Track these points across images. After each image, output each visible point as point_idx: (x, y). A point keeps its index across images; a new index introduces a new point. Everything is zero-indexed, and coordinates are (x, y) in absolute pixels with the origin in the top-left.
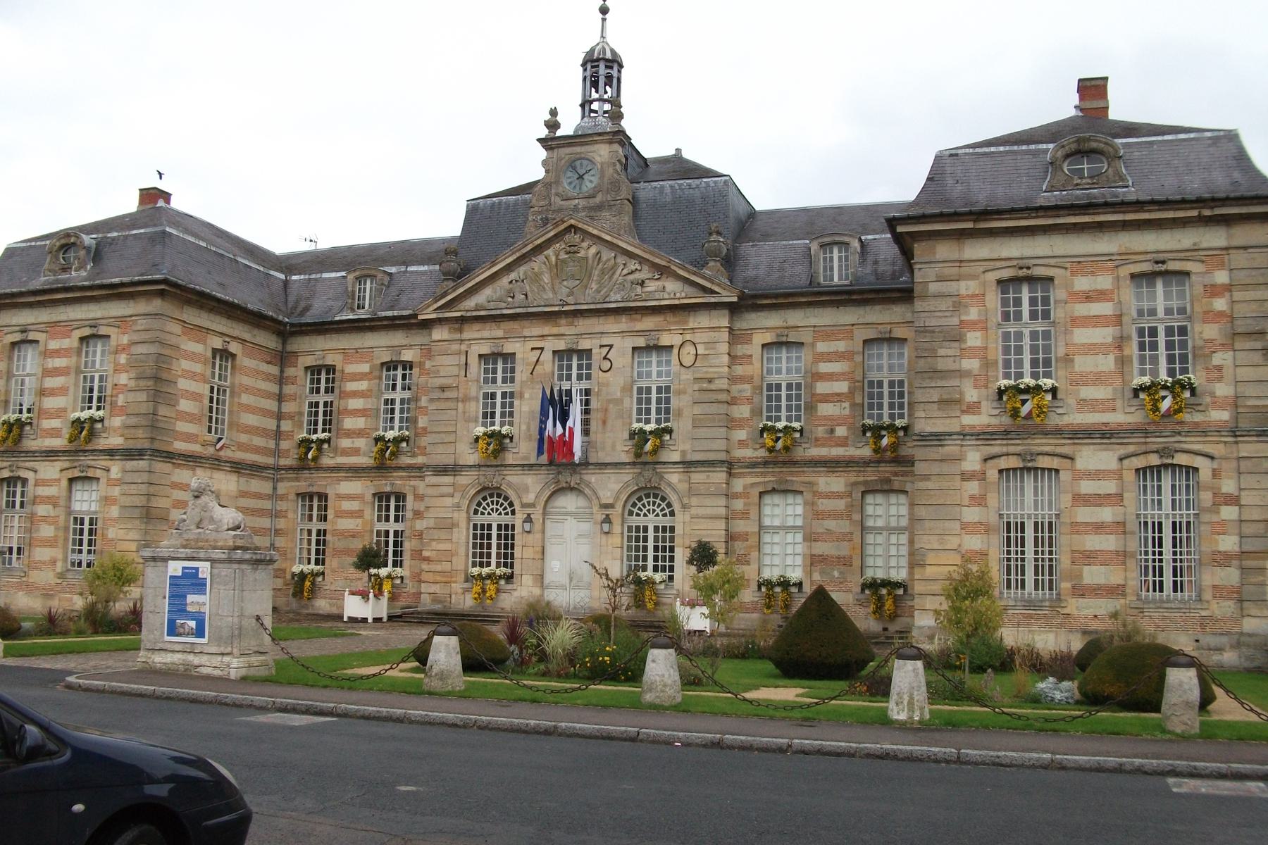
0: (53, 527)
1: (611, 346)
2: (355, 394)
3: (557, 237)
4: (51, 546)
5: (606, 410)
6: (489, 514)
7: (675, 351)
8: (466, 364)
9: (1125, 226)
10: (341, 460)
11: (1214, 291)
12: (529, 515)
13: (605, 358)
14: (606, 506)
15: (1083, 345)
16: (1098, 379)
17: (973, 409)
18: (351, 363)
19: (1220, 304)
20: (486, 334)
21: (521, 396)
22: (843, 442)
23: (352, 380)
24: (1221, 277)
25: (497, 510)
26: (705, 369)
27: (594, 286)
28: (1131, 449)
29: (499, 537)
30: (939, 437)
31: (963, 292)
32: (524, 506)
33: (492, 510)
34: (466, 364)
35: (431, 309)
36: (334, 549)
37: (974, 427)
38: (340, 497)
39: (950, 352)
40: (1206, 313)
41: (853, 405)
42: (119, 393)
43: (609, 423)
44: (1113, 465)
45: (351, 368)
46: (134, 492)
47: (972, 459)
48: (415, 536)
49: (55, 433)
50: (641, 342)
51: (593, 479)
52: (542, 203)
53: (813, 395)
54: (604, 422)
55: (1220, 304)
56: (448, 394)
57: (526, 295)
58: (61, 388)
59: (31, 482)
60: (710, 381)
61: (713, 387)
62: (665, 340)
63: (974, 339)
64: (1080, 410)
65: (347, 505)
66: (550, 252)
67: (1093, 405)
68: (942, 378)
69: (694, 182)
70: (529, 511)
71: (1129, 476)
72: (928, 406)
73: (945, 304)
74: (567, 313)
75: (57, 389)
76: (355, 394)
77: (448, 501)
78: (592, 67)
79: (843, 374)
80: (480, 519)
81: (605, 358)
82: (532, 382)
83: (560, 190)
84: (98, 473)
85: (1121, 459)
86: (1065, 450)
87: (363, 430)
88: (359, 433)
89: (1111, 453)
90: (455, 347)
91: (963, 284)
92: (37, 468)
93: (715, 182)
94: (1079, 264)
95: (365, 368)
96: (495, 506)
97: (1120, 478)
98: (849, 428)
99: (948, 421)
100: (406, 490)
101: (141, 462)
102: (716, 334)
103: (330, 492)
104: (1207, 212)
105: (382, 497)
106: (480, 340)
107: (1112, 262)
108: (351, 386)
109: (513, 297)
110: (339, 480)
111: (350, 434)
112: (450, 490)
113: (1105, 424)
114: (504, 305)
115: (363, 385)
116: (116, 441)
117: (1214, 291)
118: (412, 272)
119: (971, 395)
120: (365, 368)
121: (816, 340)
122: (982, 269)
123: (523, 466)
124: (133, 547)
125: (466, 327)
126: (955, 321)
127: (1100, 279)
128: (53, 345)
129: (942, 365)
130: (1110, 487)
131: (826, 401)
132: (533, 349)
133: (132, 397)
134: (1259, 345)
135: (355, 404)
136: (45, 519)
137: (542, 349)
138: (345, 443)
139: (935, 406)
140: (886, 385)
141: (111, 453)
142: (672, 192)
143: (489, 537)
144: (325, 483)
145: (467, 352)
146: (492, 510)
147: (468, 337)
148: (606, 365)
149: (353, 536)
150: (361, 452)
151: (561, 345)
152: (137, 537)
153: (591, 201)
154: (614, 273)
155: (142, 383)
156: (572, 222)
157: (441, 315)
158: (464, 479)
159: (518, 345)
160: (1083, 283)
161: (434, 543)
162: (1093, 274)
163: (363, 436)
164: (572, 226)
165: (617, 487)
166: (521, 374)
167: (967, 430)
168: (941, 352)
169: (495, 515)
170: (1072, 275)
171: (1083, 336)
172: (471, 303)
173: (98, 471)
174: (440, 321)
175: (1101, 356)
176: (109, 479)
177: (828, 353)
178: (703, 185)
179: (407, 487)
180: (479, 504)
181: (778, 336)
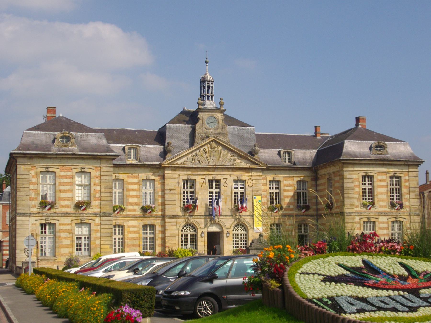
0: (69, 241)
1: (227, 179)
2: (133, 190)
3: (209, 143)
4: (69, 247)
5: (226, 199)
6: (187, 231)
7: (247, 182)
8: (178, 182)
9: (389, 165)
10: (129, 213)
11: (406, 181)
12: (202, 232)
13: (225, 183)
14: (228, 228)
15: (380, 192)
16: (383, 200)
17: (357, 207)
18: (130, 178)
19: (407, 184)
20: (185, 172)
21: (198, 193)
22: (292, 210)
23: (131, 185)
24: (407, 178)
25: (190, 230)
26: (256, 188)
27: (221, 159)
28: (390, 217)
29: (191, 239)
30: (350, 214)
31: (354, 178)
32: (201, 228)
33: (188, 230)
34: (178, 182)
35: (167, 163)
36: (128, 245)
37: (357, 211)
38: (129, 226)
39: (352, 193)
40: (404, 186)
41: (295, 199)
42: (97, 193)
43: (227, 203)
44: (387, 220)
45: (130, 181)
46: (107, 228)
47: (357, 219)
48: (159, 239)
49: (68, 206)
50: (236, 178)
51: (223, 220)
52: (200, 130)
53: (284, 196)
54: (226, 202)
55: (407, 184)
56: (172, 192)
57: (199, 161)
58: (69, 190)
59: (57, 225)
60: (257, 191)
61: (258, 193)
62: (243, 178)
63: (357, 190)
64: (380, 207)
65: (132, 229)
66: (206, 147)
67: (381, 206)
68: (350, 199)
69: (244, 128)
70: (203, 230)
71: (390, 223)
72: (348, 206)
73: (351, 181)
74: (212, 168)
75: (66, 190)
76: (133, 190)
77: (175, 227)
78: (208, 83)
79: (291, 190)
80: (184, 233)
81: (225, 183)
82: (202, 189)
83: (205, 126)
84: (90, 221)
85: (388, 219)
86: (377, 217)
87: (136, 203)
88: (136, 204)
89: (385, 218)
90: (174, 176)
91: (354, 176)
92: (59, 219)
93: (251, 129)
94: (379, 172)
95: (136, 181)
96: (189, 229)
97: (388, 223)
98: (294, 206)
99: (352, 209)
100: (155, 224)
101: (109, 217)
102: (259, 177)
103: (126, 224)
104: (406, 163)
105: (145, 226)
106: (184, 175)
107: (386, 173)
108: (131, 187)
109: (194, 161)
110: (129, 220)
111: (131, 204)
112: (175, 224)
113: (385, 211)
114: (191, 164)
115: (136, 187)
116: (97, 210)
117: (406, 181)
118: (148, 147)
119: (356, 203)
120: (136, 181)
121: (284, 180)
122: (358, 172)
123: (200, 216)
124: (108, 246)
125: (177, 169)
126: (353, 185)
127: (383, 176)
128: (63, 174)
129: (350, 196)
130: (386, 225)
131: (287, 198)
132: (201, 178)
133: (103, 195)
134: (414, 194)
135: (132, 193)
136: (65, 238)
137: (205, 179)
138: (130, 207)
139: (349, 206)
140: (302, 194)
141: (95, 214)
142: (237, 130)
143: (187, 239)
144: (123, 221)
145: (178, 178)
146: (188, 230)
147: (179, 173)
148: (226, 185)
149: (135, 240)
150: (137, 210)
151: (211, 178)
152: (110, 243)
153: (216, 131)
154: (227, 156)
155: (107, 190)
156: (213, 139)
157: (171, 166)
158: (179, 220)
159: (196, 177)
160: (380, 177)
161: (170, 241)
162: (382, 175)
163: (137, 205)
164: (214, 140)
165: (231, 223)
166: (198, 186)
167: (356, 212)
168: (350, 192)
169: (189, 232)
170: (378, 175)
171: (380, 190)
172: (179, 162)
173: (90, 220)
174: (169, 167)
175: (384, 195)
176: (95, 223)
177: (287, 184)
178: (247, 129)
179: (156, 223)
180: (183, 228)
181: (273, 178)
